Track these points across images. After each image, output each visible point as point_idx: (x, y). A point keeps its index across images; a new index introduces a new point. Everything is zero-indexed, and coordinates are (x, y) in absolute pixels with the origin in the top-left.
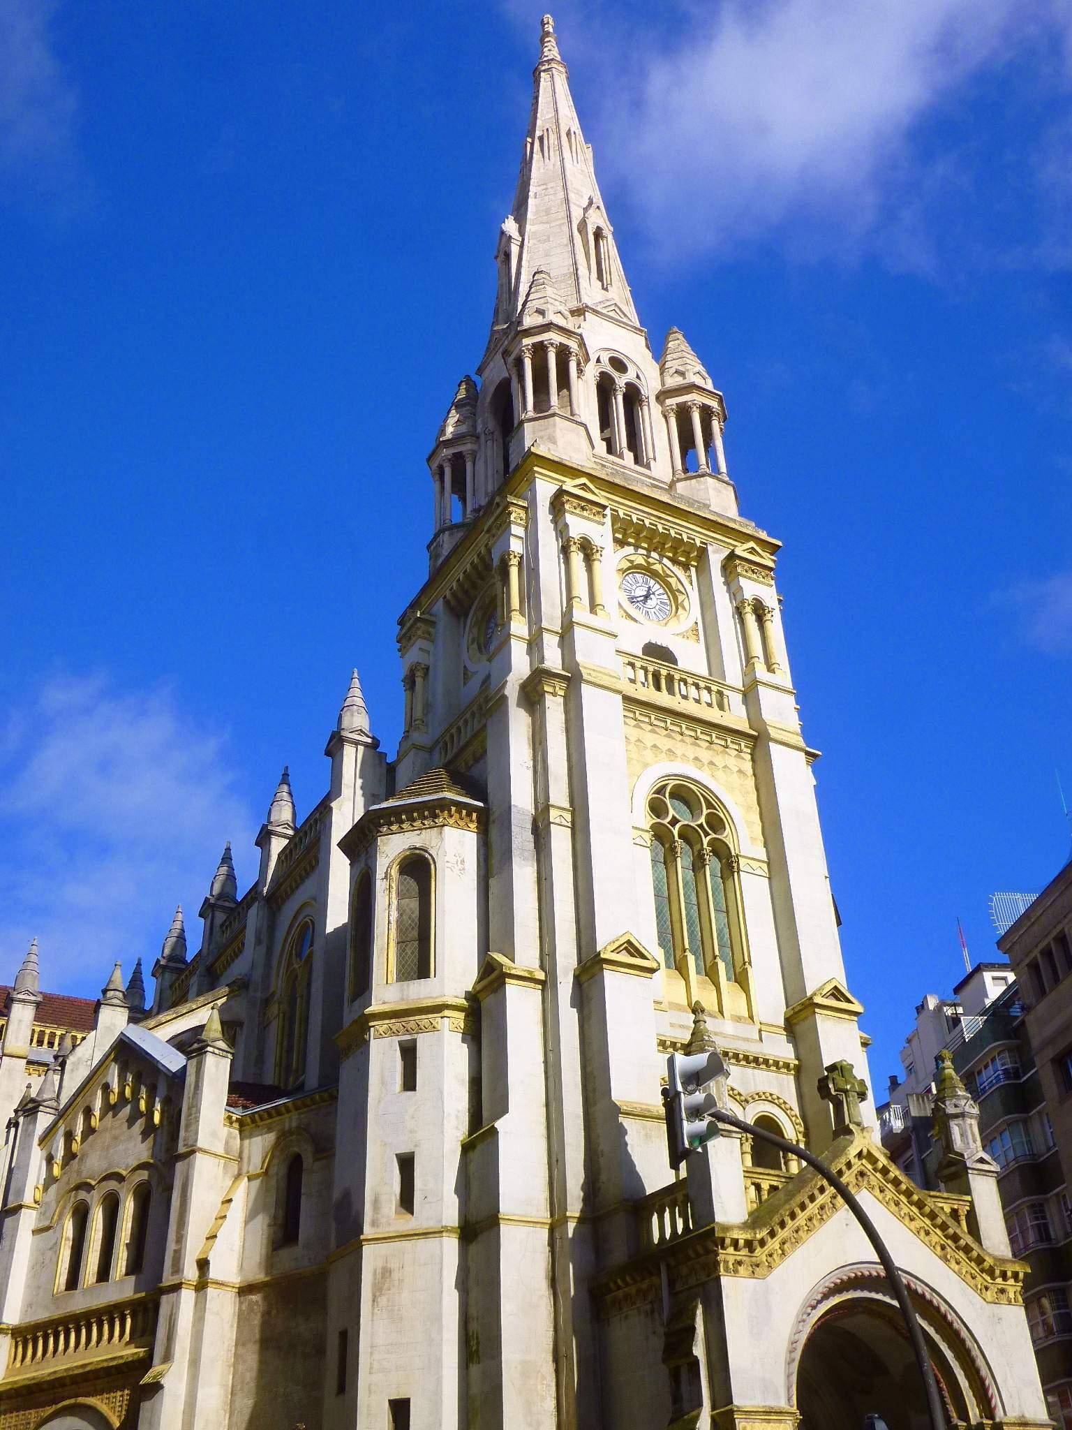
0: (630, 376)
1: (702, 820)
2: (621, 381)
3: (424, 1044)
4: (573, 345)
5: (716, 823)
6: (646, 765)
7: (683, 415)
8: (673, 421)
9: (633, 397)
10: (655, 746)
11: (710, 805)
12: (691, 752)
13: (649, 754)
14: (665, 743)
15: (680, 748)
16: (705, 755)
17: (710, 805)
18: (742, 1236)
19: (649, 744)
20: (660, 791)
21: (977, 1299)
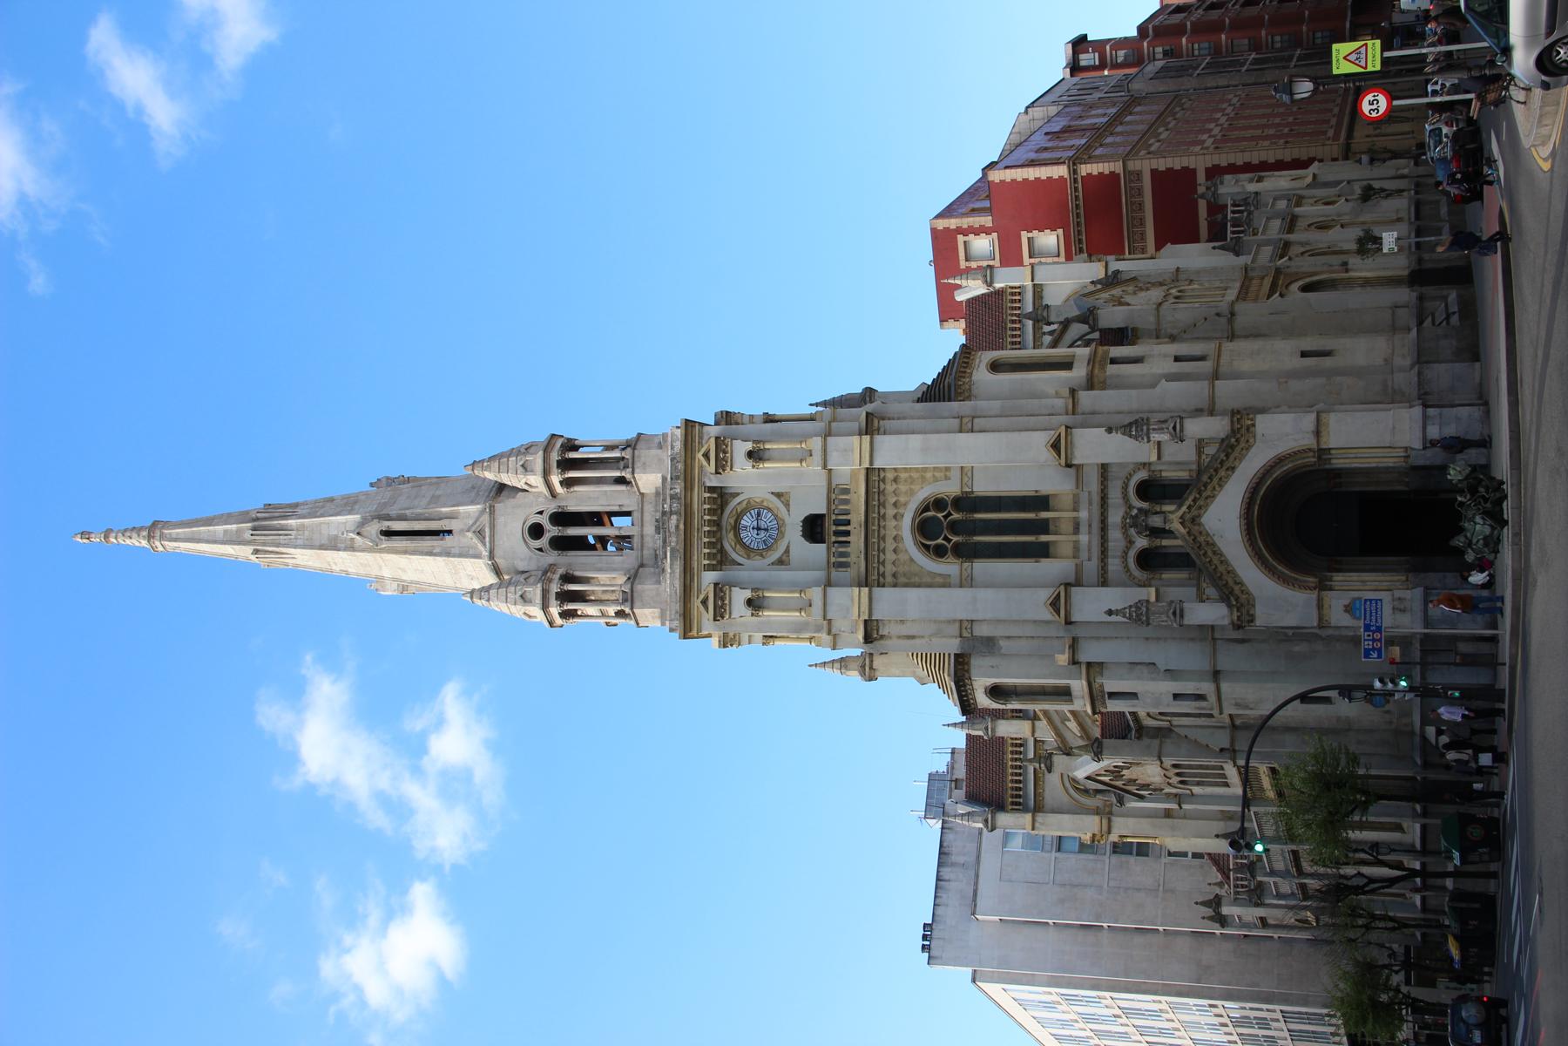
0: (544, 520)
1: (940, 515)
2: (552, 531)
3: (1108, 689)
4: (555, 588)
5: (939, 504)
6: (912, 560)
7: (568, 483)
8: (576, 488)
9: (561, 518)
10: (895, 551)
11: (926, 509)
12: (891, 523)
13: (903, 557)
14: (890, 545)
15: (890, 533)
16: (890, 512)
17: (926, 509)
18: (1236, 614)
19: (894, 557)
20: (927, 547)
21: (1253, 450)
